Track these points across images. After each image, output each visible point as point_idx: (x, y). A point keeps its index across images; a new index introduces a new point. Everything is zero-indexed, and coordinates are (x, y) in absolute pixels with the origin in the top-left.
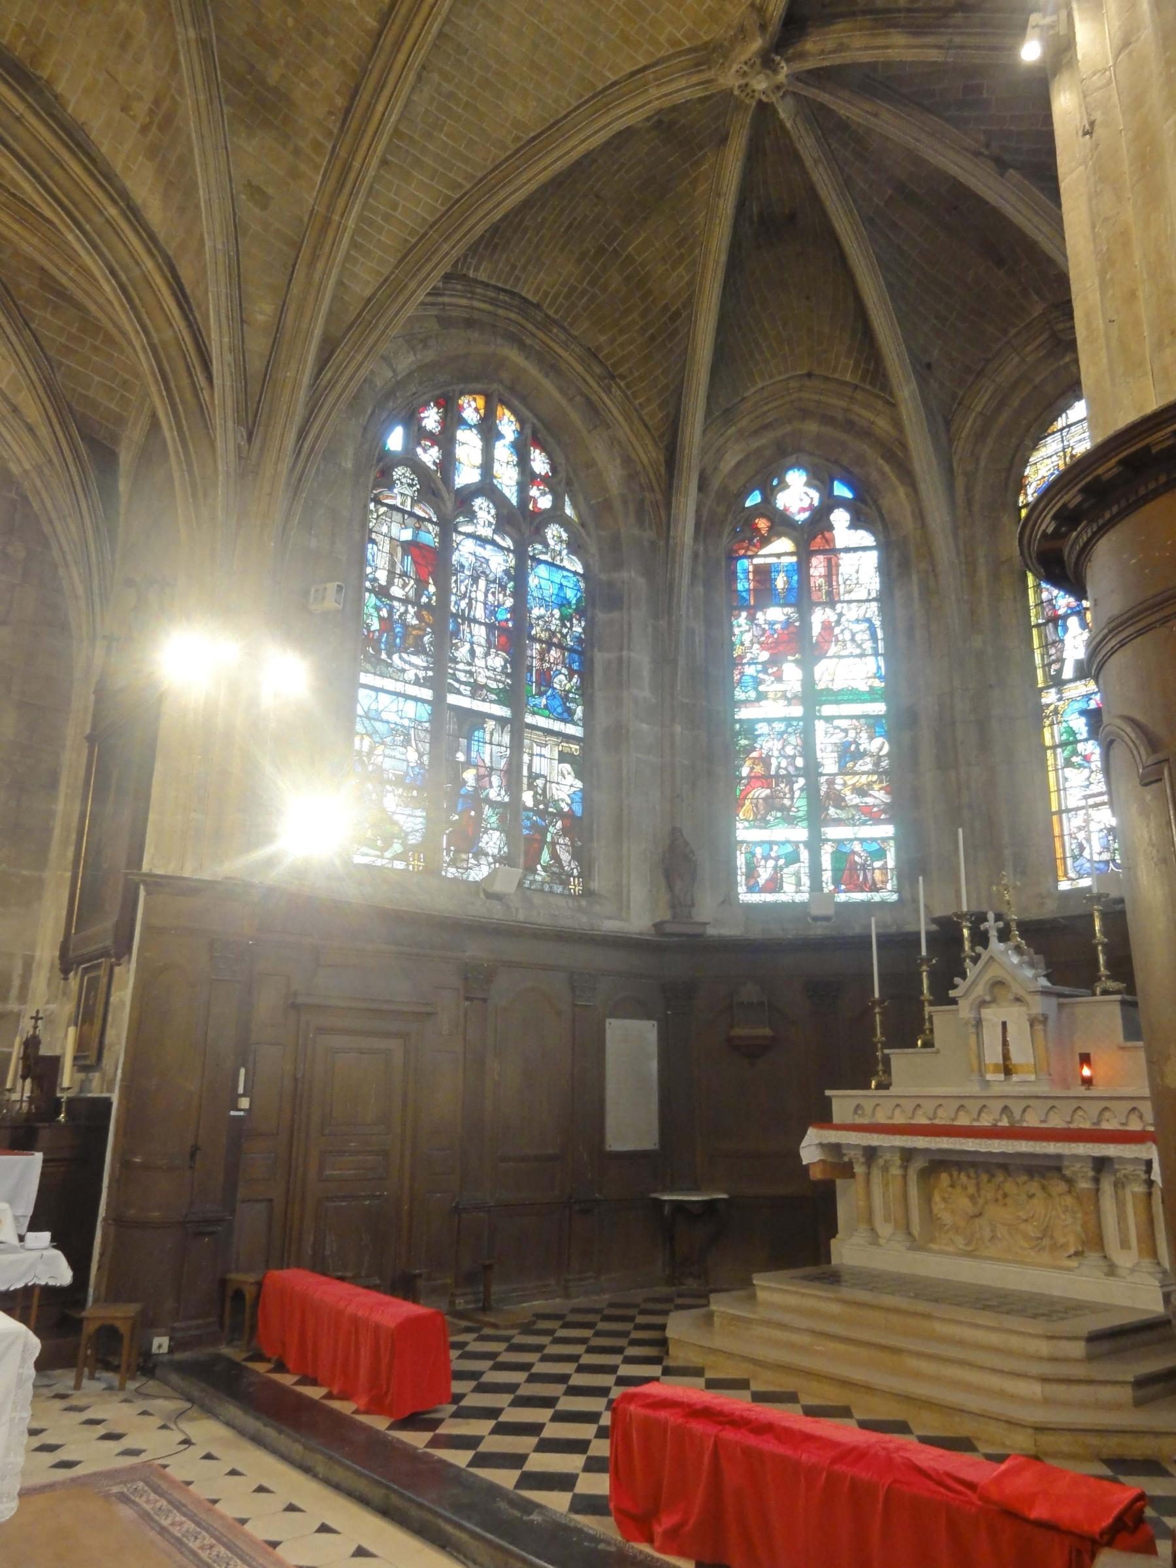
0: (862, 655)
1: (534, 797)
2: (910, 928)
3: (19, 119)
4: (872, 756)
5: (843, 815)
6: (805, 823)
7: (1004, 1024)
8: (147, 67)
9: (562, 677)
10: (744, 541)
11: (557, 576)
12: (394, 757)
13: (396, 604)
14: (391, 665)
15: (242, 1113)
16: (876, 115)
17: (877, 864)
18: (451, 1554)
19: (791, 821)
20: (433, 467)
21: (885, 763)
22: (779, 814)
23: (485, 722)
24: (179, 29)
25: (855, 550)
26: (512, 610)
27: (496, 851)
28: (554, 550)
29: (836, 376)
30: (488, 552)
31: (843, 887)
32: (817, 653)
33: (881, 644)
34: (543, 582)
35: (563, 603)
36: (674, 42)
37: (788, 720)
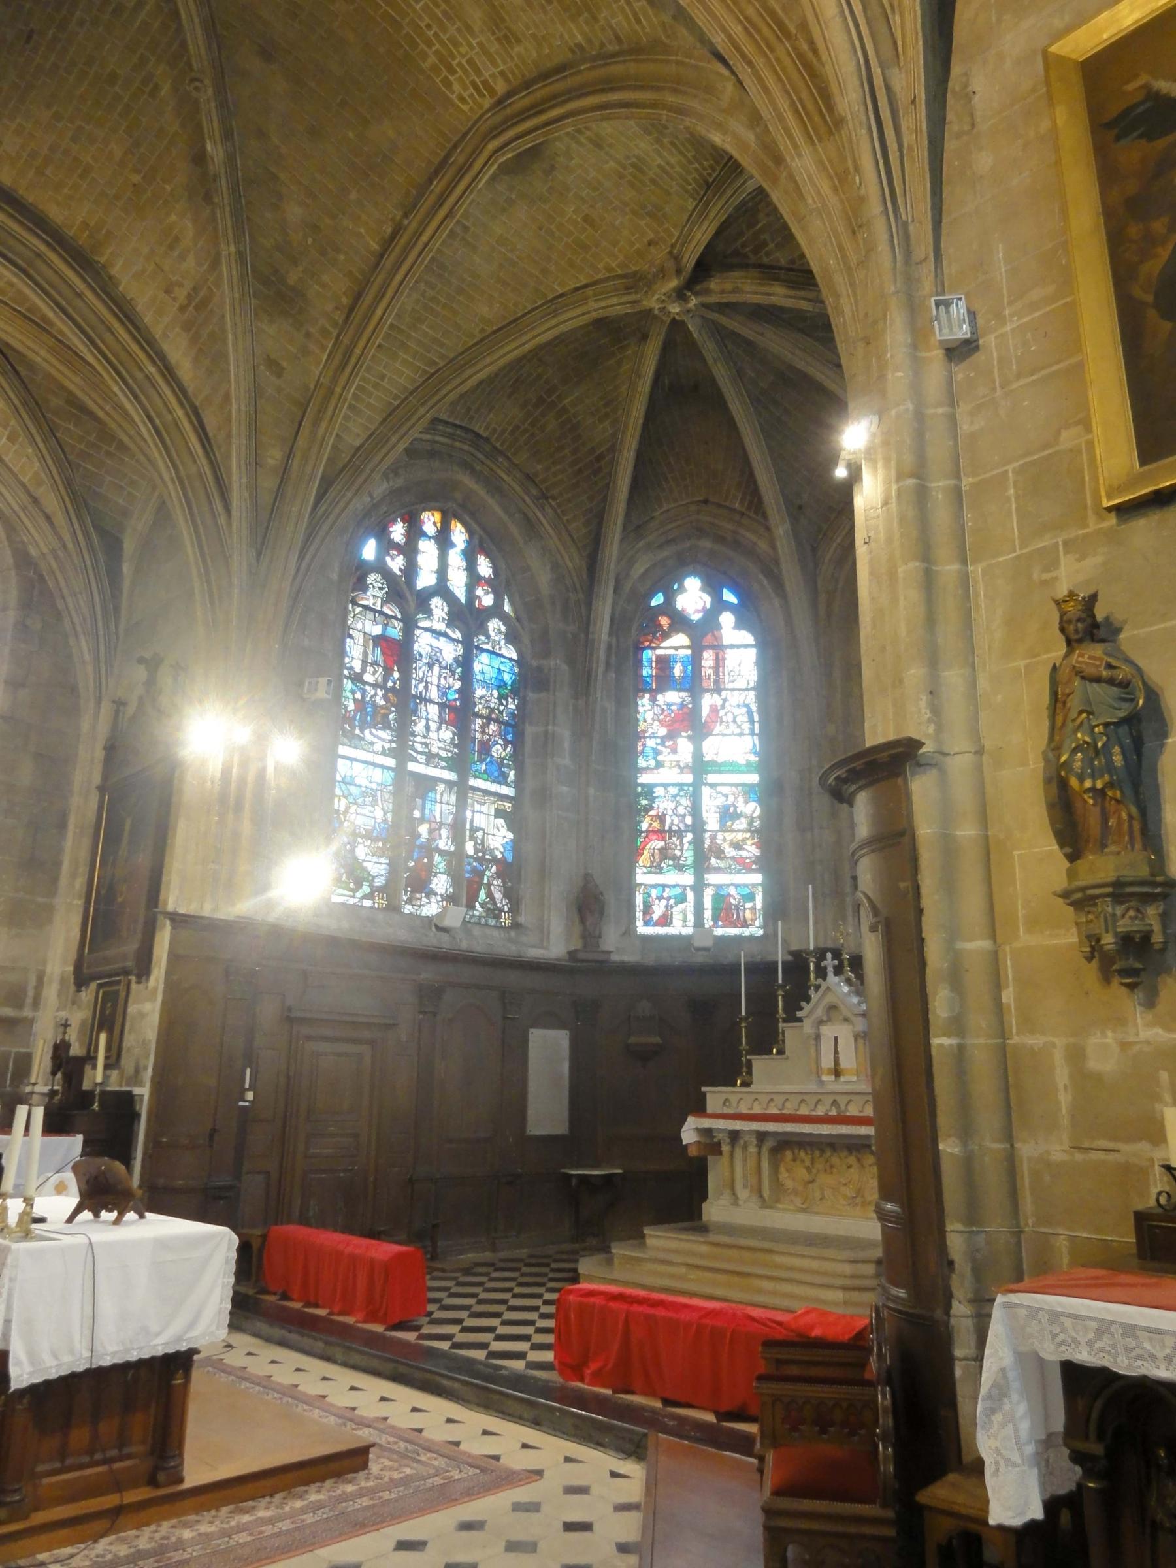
0: (741, 734)
1: (475, 846)
2: (770, 958)
3: (79, 295)
4: (746, 817)
5: (722, 864)
6: (692, 870)
7: (836, 1038)
8: (190, 263)
9: (498, 747)
10: (649, 634)
11: (497, 662)
12: (364, 815)
13: (368, 688)
14: (363, 739)
15: (247, 1104)
16: (762, 334)
17: (748, 905)
18: (446, 1398)
19: (680, 868)
20: (399, 573)
21: (757, 823)
22: (671, 863)
23: (437, 785)
24: (223, 246)
25: (739, 647)
26: (460, 691)
27: (443, 892)
28: (494, 640)
29: (727, 504)
30: (442, 643)
31: (720, 923)
32: (705, 731)
33: (756, 725)
34: (485, 667)
35: (501, 685)
36: (609, 269)
37: (681, 786)
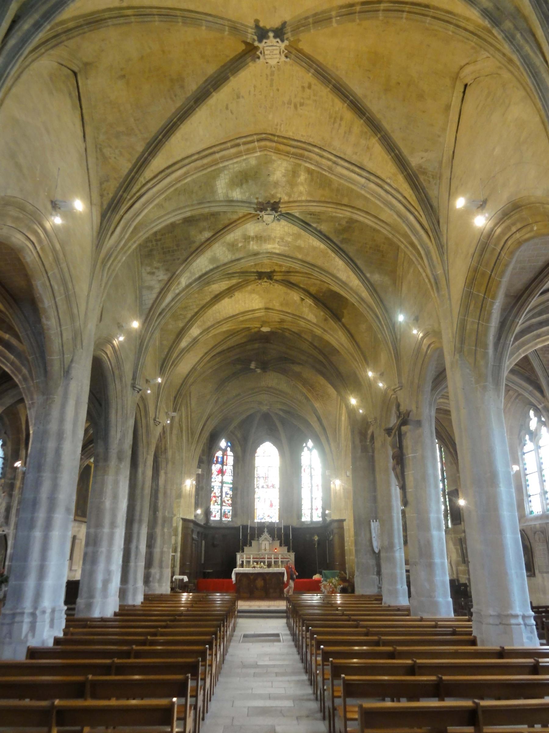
19: (218, 505)
